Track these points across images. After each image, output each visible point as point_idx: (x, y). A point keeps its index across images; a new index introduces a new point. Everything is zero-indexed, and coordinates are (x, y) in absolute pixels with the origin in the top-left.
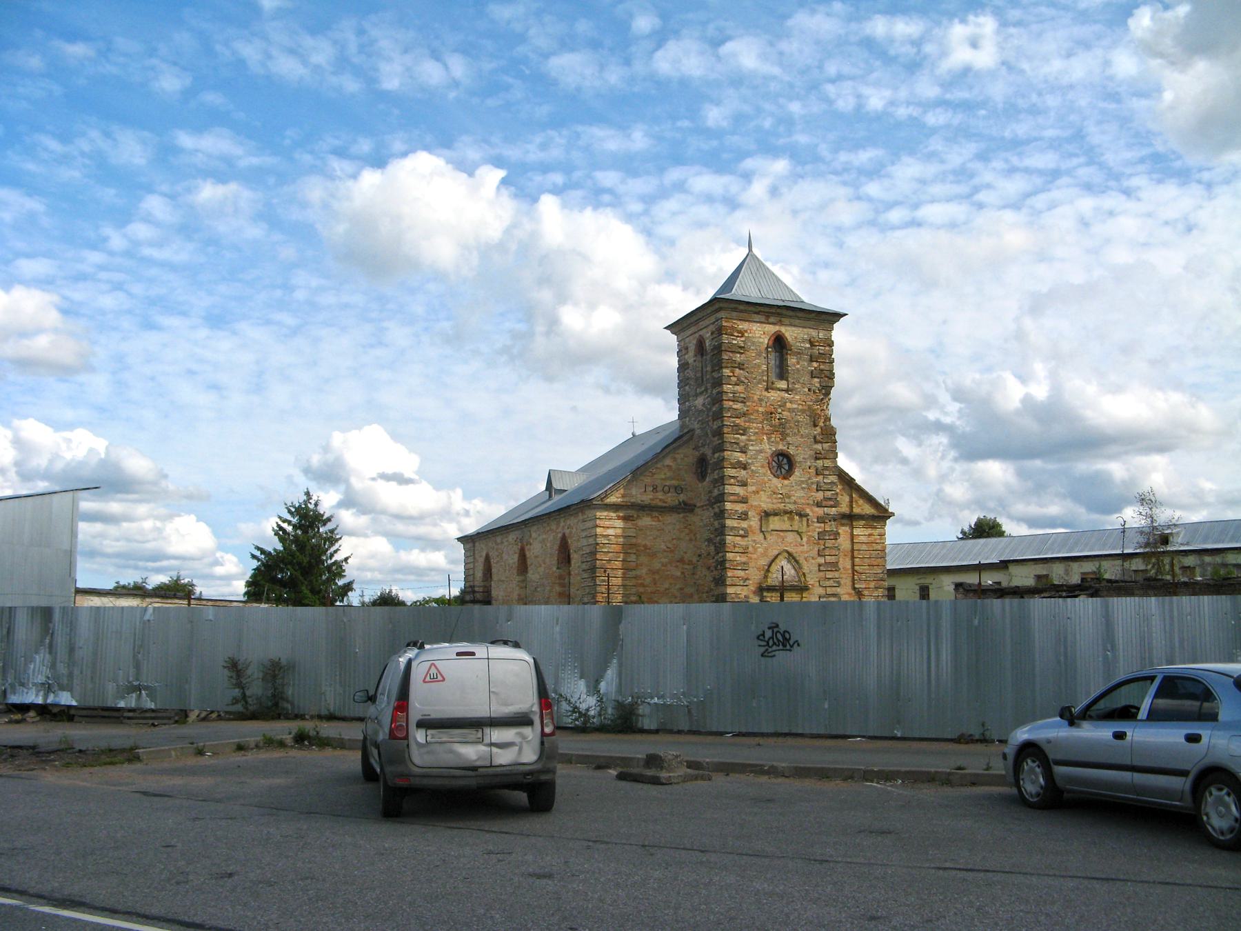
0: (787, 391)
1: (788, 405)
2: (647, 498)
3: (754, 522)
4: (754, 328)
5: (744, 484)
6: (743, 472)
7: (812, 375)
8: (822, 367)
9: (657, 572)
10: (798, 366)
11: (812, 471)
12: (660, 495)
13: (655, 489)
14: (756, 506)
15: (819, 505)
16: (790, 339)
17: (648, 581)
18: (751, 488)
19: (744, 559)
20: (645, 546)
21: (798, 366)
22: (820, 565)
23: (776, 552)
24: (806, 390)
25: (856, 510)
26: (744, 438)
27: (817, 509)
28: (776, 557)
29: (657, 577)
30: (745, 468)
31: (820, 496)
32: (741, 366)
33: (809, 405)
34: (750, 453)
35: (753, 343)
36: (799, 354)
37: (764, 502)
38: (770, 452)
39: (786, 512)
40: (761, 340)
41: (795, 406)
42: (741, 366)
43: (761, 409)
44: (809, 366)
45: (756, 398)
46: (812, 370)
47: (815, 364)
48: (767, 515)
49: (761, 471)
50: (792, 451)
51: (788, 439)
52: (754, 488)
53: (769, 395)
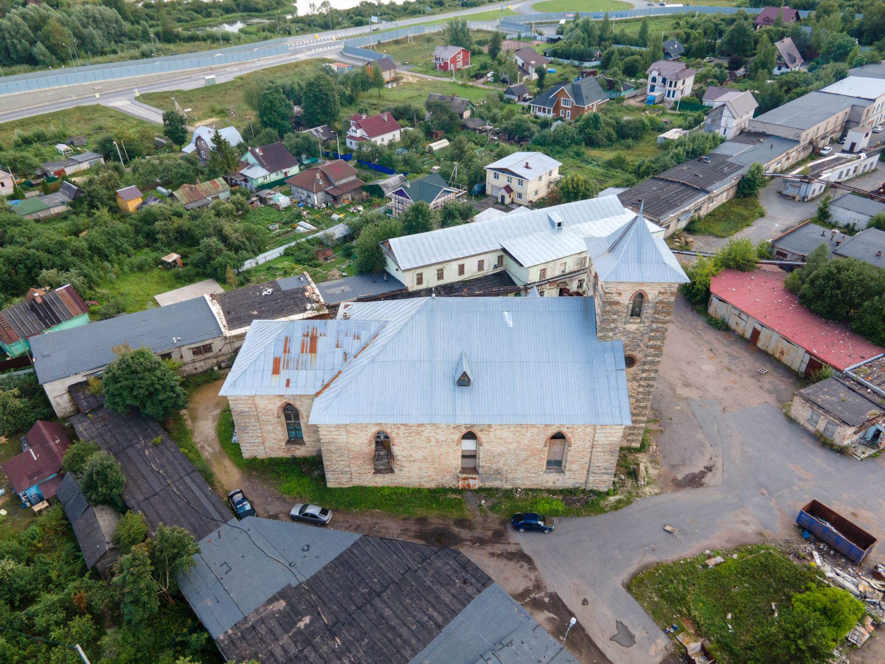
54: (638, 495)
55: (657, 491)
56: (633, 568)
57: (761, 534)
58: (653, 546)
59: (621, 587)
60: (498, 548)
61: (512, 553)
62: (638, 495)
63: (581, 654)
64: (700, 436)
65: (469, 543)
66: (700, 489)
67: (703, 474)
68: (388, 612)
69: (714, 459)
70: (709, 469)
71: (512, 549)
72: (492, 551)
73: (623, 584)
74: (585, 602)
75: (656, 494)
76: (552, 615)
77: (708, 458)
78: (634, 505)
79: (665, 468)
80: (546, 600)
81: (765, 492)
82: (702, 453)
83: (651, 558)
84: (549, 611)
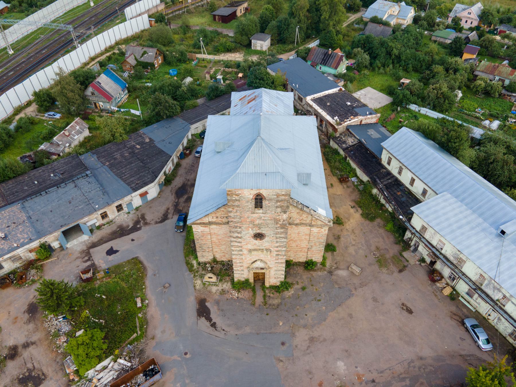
0: (263, 213)
1: (263, 218)
2: (214, 220)
3: (245, 252)
4: (245, 193)
5: (239, 242)
6: (239, 240)
7: (277, 207)
8: (282, 204)
9: (221, 239)
10: (269, 205)
11: (275, 238)
12: (220, 219)
13: (217, 217)
14: (246, 248)
15: (277, 247)
16: (265, 195)
17: (216, 241)
18: (242, 244)
19: (241, 261)
20: (215, 233)
21: (269, 205)
22: (276, 263)
23: (255, 260)
24: (273, 213)
25: (313, 223)
26: (240, 229)
27: (276, 248)
28: (256, 261)
29: (220, 241)
30: (240, 238)
31: (278, 244)
32: (238, 206)
33: (274, 218)
34: (242, 234)
35: (244, 198)
36: (270, 200)
37: (250, 247)
38: (252, 233)
39: (260, 249)
40: (249, 197)
41: (266, 218)
42: (238, 206)
43: (248, 220)
44: (275, 204)
45: (246, 217)
46: (277, 206)
47: (279, 203)
48: (250, 251)
49: (248, 239)
50: (263, 232)
51: (262, 229)
52: (245, 244)
53: (251, 215)
54: (195, 276)
55: (197, 287)
56: (146, 263)
57: (153, 338)
58: (158, 275)
59: (137, 256)
60: (171, 211)
61: (167, 215)
62: (195, 276)
63: (109, 235)
64: (248, 330)
65: (177, 201)
66: (196, 314)
67: (209, 319)
68: (133, 165)
69: (223, 332)
70: (214, 325)
71: (170, 216)
72: (170, 209)
73: (138, 257)
74: (133, 240)
75: (195, 286)
76: (130, 227)
77: (224, 328)
78: (188, 272)
79: (217, 297)
80: (138, 226)
81: (188, 356)
82: (229, 326)
83: (150, 273)
84: (132, 227)
